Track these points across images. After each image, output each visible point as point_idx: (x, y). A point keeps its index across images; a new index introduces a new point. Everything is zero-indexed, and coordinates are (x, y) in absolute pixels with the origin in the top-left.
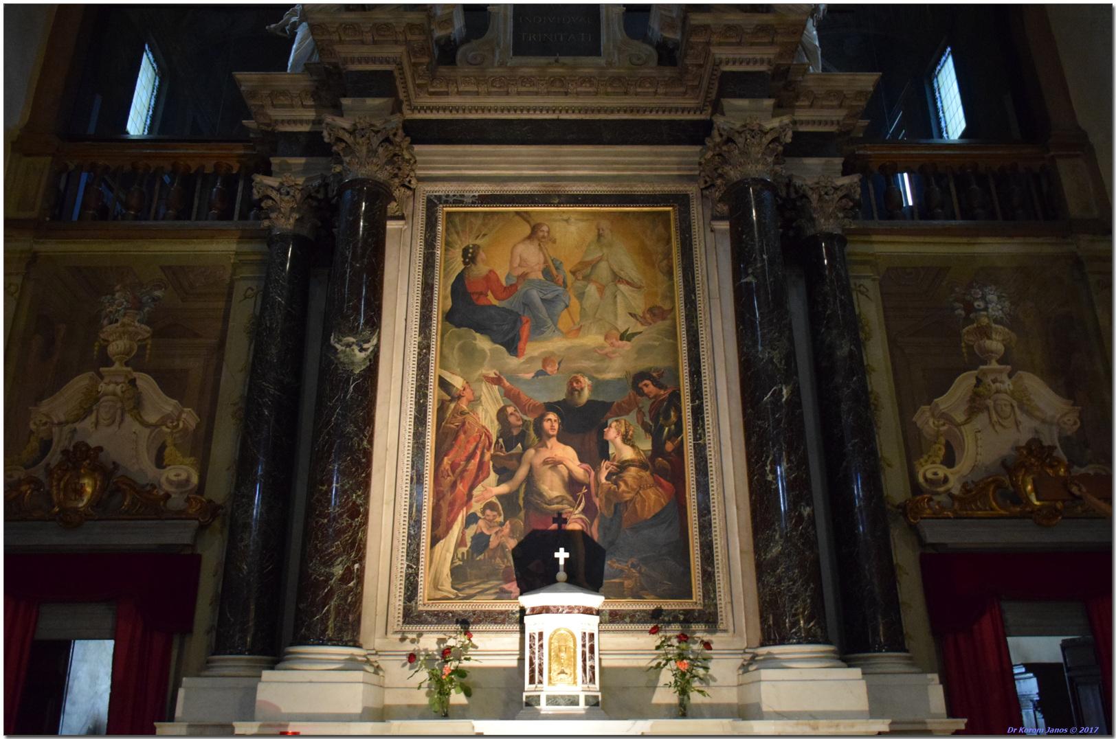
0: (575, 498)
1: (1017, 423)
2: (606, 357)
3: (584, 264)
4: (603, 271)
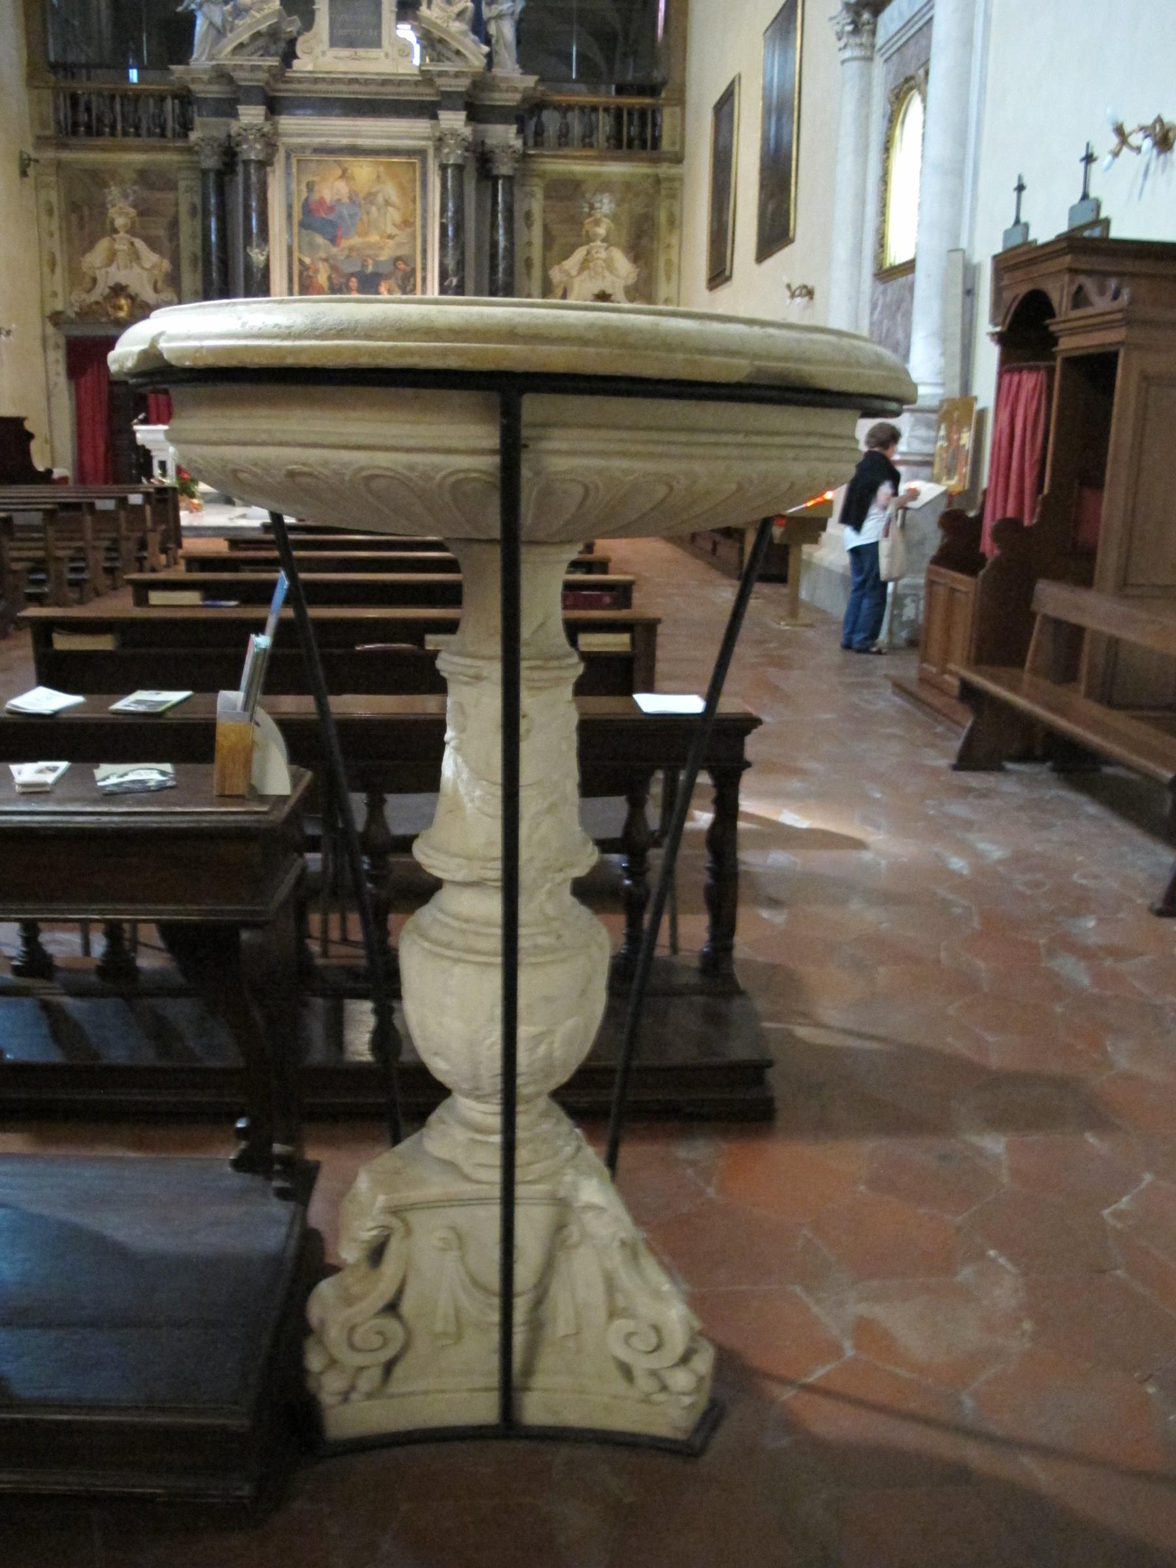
1: (604, 277)
2: (381, 248)
4: (380, 199)
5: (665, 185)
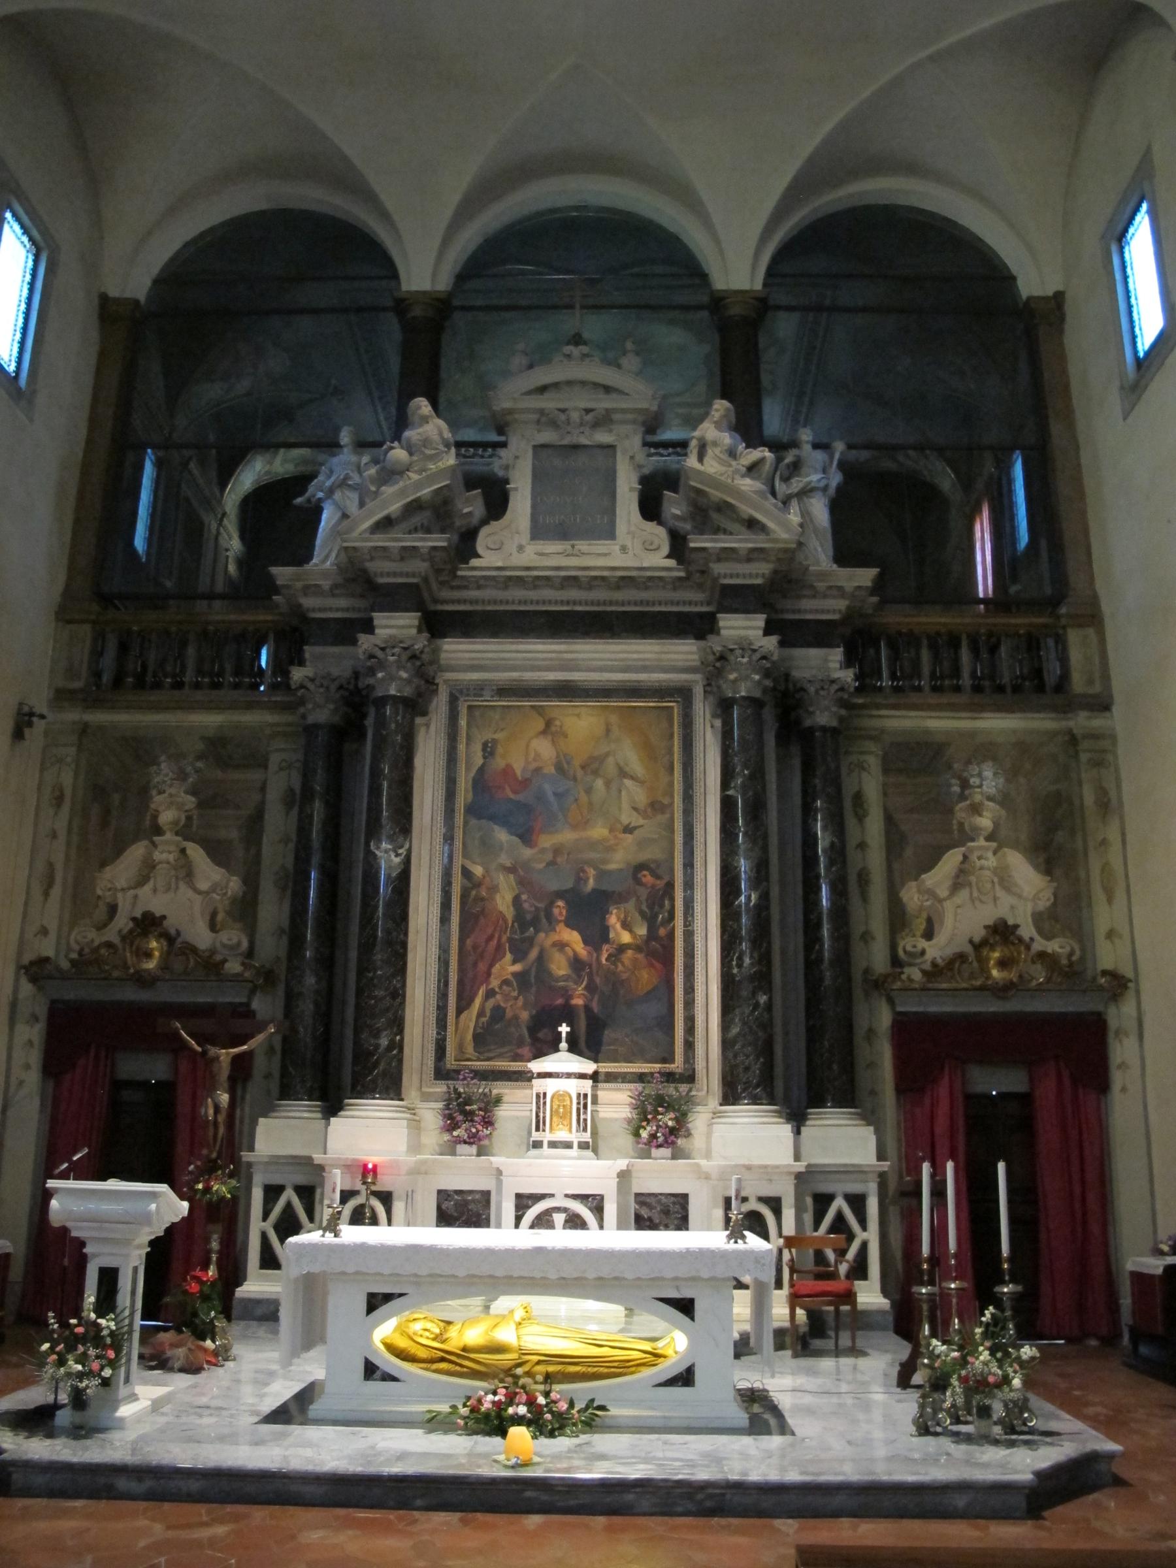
0: (579, 976)
1: (995, 899)
2: (610, 849)
3: (593, 759)
5: (1085, 745)
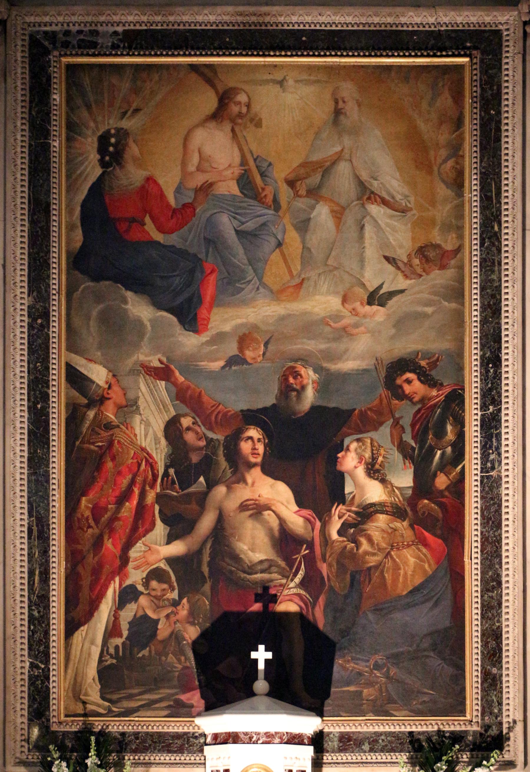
0: (290, 563)
